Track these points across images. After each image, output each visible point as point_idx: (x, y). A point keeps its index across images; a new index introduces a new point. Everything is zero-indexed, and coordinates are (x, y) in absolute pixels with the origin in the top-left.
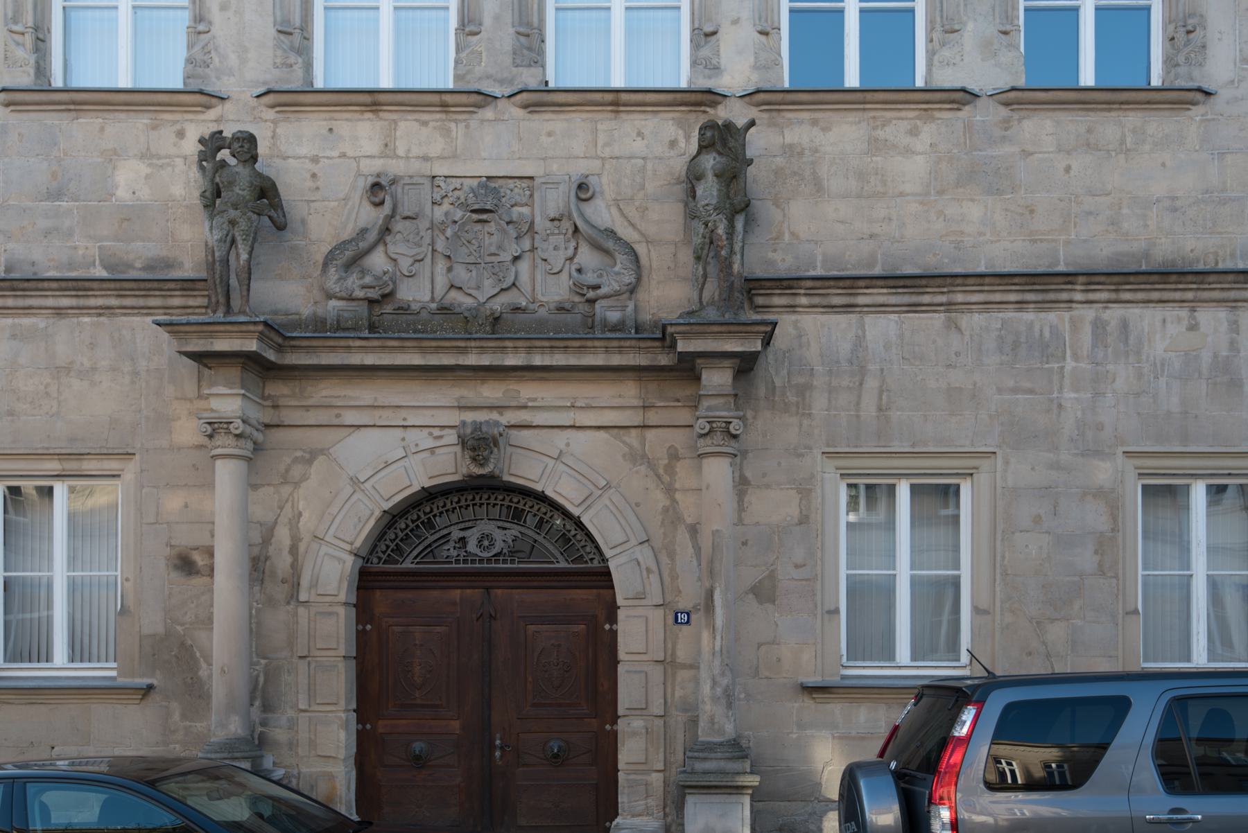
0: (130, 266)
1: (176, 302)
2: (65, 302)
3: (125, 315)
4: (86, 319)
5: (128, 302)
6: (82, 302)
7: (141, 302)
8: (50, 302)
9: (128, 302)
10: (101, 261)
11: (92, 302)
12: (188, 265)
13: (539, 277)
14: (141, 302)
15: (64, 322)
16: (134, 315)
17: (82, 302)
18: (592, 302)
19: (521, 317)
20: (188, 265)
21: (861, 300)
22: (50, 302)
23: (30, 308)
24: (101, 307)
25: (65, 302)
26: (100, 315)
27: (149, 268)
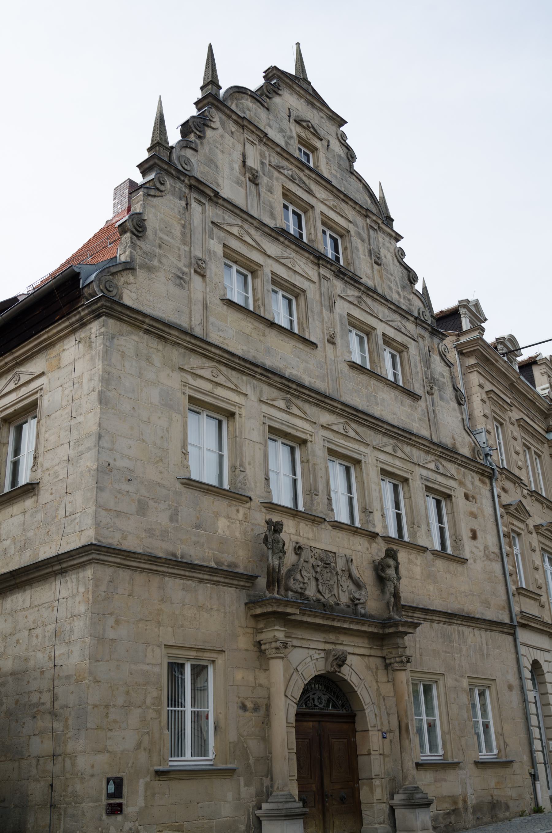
0: (223, 564)
1: (242, 583)
2: (206, 577)
3: (222, 586)
4: (209, 585)
5: (227, 581)
6: (212, 578)
7: (231, 581)
8: (201, 576)
9: (227, 581)
10: (214, 559)
11: (215, 579)
12: (241, 567)
13: (340, 591)
14: (231, 581)
15: (202, 585)
16: (225, 586)
17: (212, 578)
18: (356, 605)
19: (337, 607)
20: (241, 567)
21: (415, 615)
22: (201, 576)
23: (193, 577)
24: (217, 581)
25: (206, 577)
26: (214, 584)
27: (229, 566)
